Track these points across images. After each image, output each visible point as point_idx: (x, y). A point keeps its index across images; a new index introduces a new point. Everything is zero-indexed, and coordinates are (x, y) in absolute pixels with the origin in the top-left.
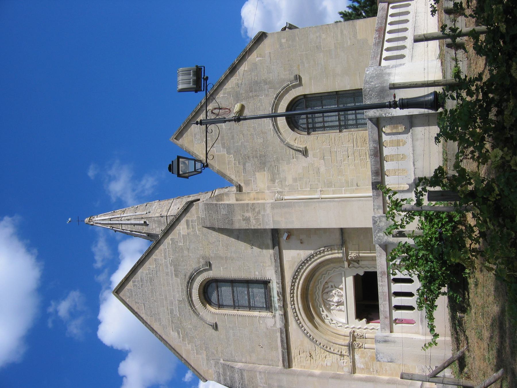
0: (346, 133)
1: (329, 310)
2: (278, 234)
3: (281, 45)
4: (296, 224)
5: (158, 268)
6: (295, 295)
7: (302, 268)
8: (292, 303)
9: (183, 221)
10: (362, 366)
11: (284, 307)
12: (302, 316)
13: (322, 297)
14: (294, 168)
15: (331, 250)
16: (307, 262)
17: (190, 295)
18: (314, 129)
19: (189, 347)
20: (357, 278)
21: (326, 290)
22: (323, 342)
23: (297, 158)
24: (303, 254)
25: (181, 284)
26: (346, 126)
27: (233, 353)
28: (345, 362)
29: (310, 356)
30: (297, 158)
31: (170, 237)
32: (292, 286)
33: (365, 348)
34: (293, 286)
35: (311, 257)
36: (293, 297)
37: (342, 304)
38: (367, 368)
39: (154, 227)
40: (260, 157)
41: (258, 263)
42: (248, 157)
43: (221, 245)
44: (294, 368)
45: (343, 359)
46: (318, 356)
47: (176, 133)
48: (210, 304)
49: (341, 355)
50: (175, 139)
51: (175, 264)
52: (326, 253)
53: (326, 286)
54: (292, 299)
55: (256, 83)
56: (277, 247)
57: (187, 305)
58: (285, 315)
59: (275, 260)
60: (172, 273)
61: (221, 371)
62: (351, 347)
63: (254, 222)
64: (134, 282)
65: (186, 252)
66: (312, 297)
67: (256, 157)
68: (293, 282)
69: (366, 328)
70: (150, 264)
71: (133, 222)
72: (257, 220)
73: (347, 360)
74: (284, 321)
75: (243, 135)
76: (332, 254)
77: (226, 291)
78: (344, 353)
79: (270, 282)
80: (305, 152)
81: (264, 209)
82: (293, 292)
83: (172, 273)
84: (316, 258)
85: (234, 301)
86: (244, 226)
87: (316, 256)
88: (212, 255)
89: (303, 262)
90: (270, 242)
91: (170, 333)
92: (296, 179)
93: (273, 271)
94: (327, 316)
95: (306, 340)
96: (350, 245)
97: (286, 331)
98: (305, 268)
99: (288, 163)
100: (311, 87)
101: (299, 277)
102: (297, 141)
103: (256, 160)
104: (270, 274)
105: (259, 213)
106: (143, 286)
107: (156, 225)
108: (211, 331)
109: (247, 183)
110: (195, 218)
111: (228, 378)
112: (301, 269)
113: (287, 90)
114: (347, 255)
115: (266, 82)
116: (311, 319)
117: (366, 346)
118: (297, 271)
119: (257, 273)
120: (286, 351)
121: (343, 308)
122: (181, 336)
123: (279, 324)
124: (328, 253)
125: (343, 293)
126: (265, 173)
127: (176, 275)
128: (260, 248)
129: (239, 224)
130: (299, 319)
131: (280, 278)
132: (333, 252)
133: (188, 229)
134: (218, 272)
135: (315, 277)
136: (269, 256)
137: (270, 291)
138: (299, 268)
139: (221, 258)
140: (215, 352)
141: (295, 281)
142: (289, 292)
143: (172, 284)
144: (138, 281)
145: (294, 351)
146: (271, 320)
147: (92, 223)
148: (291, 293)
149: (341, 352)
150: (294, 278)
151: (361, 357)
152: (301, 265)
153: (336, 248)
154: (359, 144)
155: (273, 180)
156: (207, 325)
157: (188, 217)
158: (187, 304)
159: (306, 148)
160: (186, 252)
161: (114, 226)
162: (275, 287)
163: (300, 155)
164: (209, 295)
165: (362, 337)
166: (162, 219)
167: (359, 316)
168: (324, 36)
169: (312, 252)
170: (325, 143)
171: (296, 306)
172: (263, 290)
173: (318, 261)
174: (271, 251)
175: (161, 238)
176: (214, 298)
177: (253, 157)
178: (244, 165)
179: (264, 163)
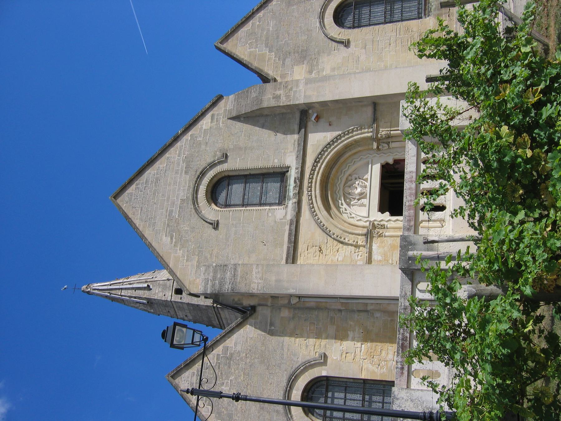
1: (349, 205)
2: (307, 118)
5: (168, 166)
6: (314, 181)
7: (327, 151)
8: (310, 189)
9: (208, 116)
10: (380, 258)
11: (300, 194)
12: (318, 204)
13: (343, 190)
14: (332, 60)
15: (361, 129)
16: (333, 144)
17: (196, 191)
18: (359, 26)
19: (180, 253)
21: (349, 183)
22: (337, 232)
23: (338, 50)
24: (329, 136)
25: (189, 181)
27: (230, 255)
28: (360, 255)
29: (320, 251)
30: (338, 50)
31: (190, 133)
32: (312, 170)
33: (385, 237)
34: (313, 170)
35: (337, 138)
36: (311, 182)
37: (365, 197)
38: (385, 260)
39: (157, 292)
40: (301, 52)
41: (278, 150)
42: (290, 53)
43: (243, 135)
45: (358, 252)
46: (328, 251)
47: (222, 35)
48: (216, 205)
50: (220, 43)
51: (188, 161)
52: (354, 133)
53: (350, 178)
54: (310, 184)
56: (303, 130)
57: (190, 204)
59: (299, 144)
60: (182, 171)
63: (284, 99)
64: (137, 185)
65: (203, 147)
66: (333, 185)
67: (298, 52)
68: (313, 166)
69: (390, 220)
70: (161, 164)
71: (135, 286)
72: (288, 97)
73: (363, 251)
74: (297, 210)
75: (289, 34)
76: (361, 134)
77: (237, 189)
78: (360, 243)
79: (288, 171)
80: (346, 44)
81: (297, 86)
82: (313, 177)
83: (182, 171)
84: (343, 139)
85: (244, 198)
86: (273, 103)
87: (344, 136)
88: (231, 147)
89: (329, 144)
90: (296, 127)
91: (161, 239)
92: (335, 68)
93: (295, 157)
94: (346, 210)
95: (319, 231)
96: (381, 124)
98: (329, 150)
99: (329, 54)
101: (321, 161)
102: (340, 35)
103: (297, 55)
104: (291, 160)
105: (291, 89)
106: (147, 188)
107: (160, 289)
108: (209, 230)
109: (282, 76)
110: (222, 111)
111: (217, 282)
112: (325, 152)
114: (377, 132)
116: (328, 208)
117: (387, 234)
118: (320, 153)
119: (276, 161)
120: (293, 244)
122: (174, 240)
124: (356, 133)
125: (368, 184)
126: (304, 66)
127: (186, 173)
128: (284, 134)
130: (313, 207)
131: (301, 162)
132: (363, 131)
133: (211, 122)
134: (234, 164)
135: (339, 163)
136: (293, 141)
137: (287, 181)
138: (323, 150)
139: (240, 149)
140: (209, 256)
141: (317, 165)
142: (308, 176)
143: (179, 182)
144: (143, 183)
146: (283, 214)
147: (89, 290)
148: (309, 178)
149: (357, 242)
150: (316, 161)
151: (379, 247)
152: (326, 147)
153: (366, 127)
154: (402, 33)
155: (310, 72)
156: (207, 224)
157: (215, 111)
158: (190, 202)
159: (349, 40)
161: (113, 292)
162: (293, 174)
163: (342, 47)
164: (217, 194)
165: (383, 227)
166: (168, 282)
167: (382, 210)
169: (340, 132)
170: (368, 34)
171: (313, 193)
172: (279, 184)
173: (345, 142)
174: (296, 136)
175: (181, 134)
176: (222, 198)
177: (294, 53)
178: (284, 60)
179: (305, 58)
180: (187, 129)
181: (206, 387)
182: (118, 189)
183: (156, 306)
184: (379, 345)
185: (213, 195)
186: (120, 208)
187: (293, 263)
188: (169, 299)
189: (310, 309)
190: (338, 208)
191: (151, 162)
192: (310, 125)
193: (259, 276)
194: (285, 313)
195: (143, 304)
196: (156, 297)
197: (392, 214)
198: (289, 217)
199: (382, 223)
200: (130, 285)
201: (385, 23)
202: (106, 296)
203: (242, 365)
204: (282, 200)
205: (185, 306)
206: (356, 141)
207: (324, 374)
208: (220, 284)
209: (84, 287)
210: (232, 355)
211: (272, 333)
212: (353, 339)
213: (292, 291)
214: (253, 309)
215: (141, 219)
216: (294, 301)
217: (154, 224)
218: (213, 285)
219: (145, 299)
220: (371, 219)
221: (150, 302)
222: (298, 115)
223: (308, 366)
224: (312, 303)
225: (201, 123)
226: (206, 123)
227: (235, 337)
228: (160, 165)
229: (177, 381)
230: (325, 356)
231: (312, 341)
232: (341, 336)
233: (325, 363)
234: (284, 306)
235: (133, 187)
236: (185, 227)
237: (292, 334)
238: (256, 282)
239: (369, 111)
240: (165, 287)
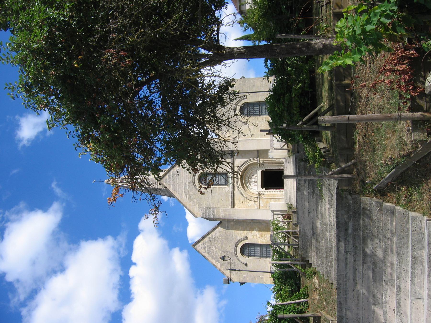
0: (261, 117)
1: (250, 185)
19: (191, 203)
20: (262, 172)
22: (248, 196)
26: (262, 115)
35: (246, 162)
37: (256, 182)
44: (235, 208)
49: (255, 201)
61: (204, 212)
62: (259, 198)
73: (257, 204)
97: (233, 193)
116: (243, 187)
121: (255, 184)
146: (228, 189)
158: (192, 183)
165: (263, 194)
167: (262, 187)
168: (256, 82)
169: (246, 160)
184: (264, 233)
188: (156, 187)
190: (247, 187)
193: (223, 213)
197: (266, 189)
199: (262, 193)
201: (260, 115)
203: (219, 241)
204: (227, 183)
206: (252, 164)
207: (247, 243)
208: (209, 215)
210: (215, 237)
211: (228, 229)
212: (256, 231)
213: (234, 218)
215: (173, 189)
218: (206, 215)
223: (242, 240)
229: (195, 247)
230: (247, 237)
231: (242, 232)
232: (252, 229)
233: (247, 239)
234: (232, 221)
235: (167, 176)
236: (191, 193)
237: (236, 229)
238: (222, 215)
239: (256, 153)
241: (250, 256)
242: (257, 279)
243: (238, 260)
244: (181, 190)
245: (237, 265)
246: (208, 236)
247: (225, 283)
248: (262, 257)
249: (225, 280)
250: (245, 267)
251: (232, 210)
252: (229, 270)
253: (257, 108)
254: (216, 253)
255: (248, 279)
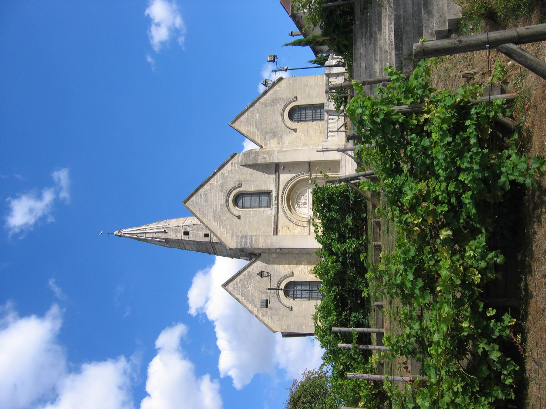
0: (315, 122)
1: (299, 207)
3: (290, 83)
4: (289, 160)
9: (230, 163)
14: (289, 138)
18: (301, 121)
19: (223, 230)
22: (295, 221)
24: (289, 176)
26: (315, 120)
31: (221, 171)
35: (293, 178)
37: (306, 204)
41: (265, 182)
47: (232, 120)
49: (304, 227)
51: (222, 185)
55: (276, 99)
58: (278, 207)
65: (229, 179)
66: (292, 199)
71: (155, 231)
72: (270, 158)
73: (307, 229)
77: (247, 199)
78: (305, 225)
80: (295, 131)
86: (263, 161)
88: (243, 180)
90: (274, 172)
100: (301, 102)
104: (272, 187)
107: (173, 233)
108: (236, 219)
109: (266, 145)
113: (290, 103)
115: (280, 99)
116: (290, 209)
123: (274, 212)
129: (260, 160)
134: (245, 188)
139: (248, 181)
145: (280, 227)
146: (270, 212)
155: (279, 143)
157: (233, 161)
158: (225, 206)
160: (229, 179)
162: (274, 194)
163: (293, 132)
168: (309, 80)
169: (294, 175)
174: (274, 176)
176: (240, 203)
178: (265, 136)
180: (219, 170)
181: (272, 287)
182: (186, 198)
183: (170, 243)
185: (236, 202)
186: (188, 208)
187: (277, 235)
188: (180, 238)
189: (285, 253)
190: (295, 209)
191: (202, 185)
192: (280, 171)
194: (274, 256)
195: (162, 242)
196: (171, 238)
198: (273, 214)
200: (151, 229)
201: (313, 120)
202: (134, 238)
204: (269, 205)
205: (192, 242)
207: (293, 280)
209: (116, 232)
210: (251, 274)
211: (269, 264)
212: (304, 265)
213: (278, 247)
214: (260, 254)
216: (278, 251)
217: (208, 216)
219: (164, 239)
220: (309, 214)
221: (167, 241)
222: (274, 166)
223: (286, 277)
224: (286, 251)
225: (226, 166)
226: (229, 166)
227: (252, 266)
228: (207, 187)
230: (293, 273)
231: (287, 266)
232: (299, 263)
233: (293, 276)
234: (274, 253)
235: (194, 197)
236: (224, 218)
237: (279, 263)
238: (261, 244)
239: (307, 166)
240: (176, 231)
241: (296, 298)
242: (304, 327)
243: (281, 303)
244: (211, 215)
245: (279, 309)
246: (244, 273)
247: (262, 307)
248: (312, 298)
249: (262, 302)
250: (289, 311)
251: (275, 236)
252: (269, 289)
253: (310, 112)
254: (252, 294)
255: (292, 327)
